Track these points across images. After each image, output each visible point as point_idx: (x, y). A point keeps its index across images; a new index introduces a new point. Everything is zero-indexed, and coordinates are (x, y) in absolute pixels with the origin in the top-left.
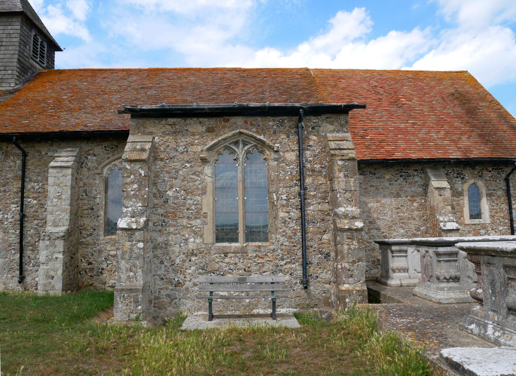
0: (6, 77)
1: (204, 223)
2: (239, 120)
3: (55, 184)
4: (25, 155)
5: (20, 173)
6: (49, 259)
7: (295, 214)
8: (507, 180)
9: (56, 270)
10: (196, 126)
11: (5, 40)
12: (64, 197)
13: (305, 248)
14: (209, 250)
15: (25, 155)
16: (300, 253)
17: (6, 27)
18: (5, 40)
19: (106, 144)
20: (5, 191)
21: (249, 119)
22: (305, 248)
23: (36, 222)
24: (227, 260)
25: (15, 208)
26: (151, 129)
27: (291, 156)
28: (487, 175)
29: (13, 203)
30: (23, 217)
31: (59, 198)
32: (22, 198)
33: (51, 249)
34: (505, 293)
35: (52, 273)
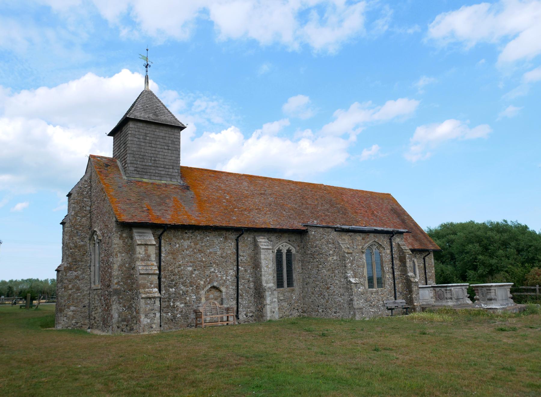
0: (174, 174)
1: (365, 280)
2: (372, 235)
3: (265, 259)
4: (237, 240)
5: (235, 250)
6: (272, 302)
7: (391, 276)
8: (424, 259)
9: (274, 308)
10: (359, 237)
11: (170, 145)
12: (270, 266)
13: (395, 290)
14: (367, 292)
15: (237, 240)
16: (393, 292)
17: (170, 136)
18: (170, 145)
19: (276, 235)
20: (226, 262)
21: (376, 235)
22: (395, 290)
23: (243, 281)
24: (372, 296)
25: (232, 273)
26: (344, 237)
27: (388, 251)
28: (418, 256)
29: (231, 269)
30: (237, 277)
31: (267, 267)
32: (238, 266)
33: (272, 296)
34: (486, 296)
35: (273, 310)
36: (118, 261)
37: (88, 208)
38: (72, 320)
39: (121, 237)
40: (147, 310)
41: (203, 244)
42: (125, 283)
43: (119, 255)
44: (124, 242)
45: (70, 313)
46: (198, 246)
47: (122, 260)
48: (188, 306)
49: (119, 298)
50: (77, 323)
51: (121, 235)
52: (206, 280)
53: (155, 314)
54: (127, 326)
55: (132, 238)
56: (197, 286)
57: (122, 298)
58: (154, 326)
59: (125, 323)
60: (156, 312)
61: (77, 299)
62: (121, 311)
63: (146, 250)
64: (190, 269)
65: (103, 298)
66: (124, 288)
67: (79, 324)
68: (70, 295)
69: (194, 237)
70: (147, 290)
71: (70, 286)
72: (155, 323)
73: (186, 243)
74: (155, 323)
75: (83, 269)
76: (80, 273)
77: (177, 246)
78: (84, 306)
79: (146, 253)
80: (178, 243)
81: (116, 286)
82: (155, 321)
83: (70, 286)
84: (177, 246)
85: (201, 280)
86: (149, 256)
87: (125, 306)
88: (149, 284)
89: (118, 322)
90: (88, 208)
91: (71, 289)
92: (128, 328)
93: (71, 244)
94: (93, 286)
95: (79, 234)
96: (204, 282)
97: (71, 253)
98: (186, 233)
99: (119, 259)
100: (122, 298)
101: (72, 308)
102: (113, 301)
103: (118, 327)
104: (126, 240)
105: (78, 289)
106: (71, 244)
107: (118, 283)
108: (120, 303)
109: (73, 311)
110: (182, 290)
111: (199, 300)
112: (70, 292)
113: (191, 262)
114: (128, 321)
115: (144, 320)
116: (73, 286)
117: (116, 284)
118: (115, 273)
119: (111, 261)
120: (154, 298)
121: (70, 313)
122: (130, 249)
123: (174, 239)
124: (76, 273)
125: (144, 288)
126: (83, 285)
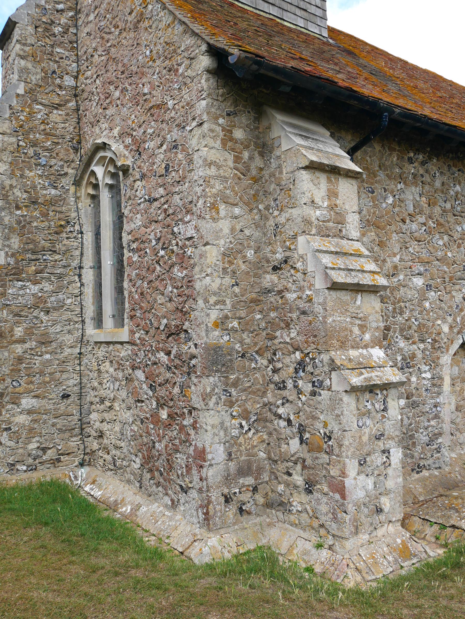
36: (216, 233)
37: (69, 81)
38: (29, 440)
39: (228, 140)
40: (365, 439)
41: (448, 206)
42: (246, 325)
43: (222, 207)
44: (237, 159)
45: (22, 419)
46: (437, 210)
47: (233, 230)
48: (414, 405)
49: (228, 385)
50: (44, 450)
51: (228, 132)
52: (455, 320)
53: (386, 452)
54: (255, 489)
55: (264, 148)
56: (435, 340)
57: (235, 384)
58: (386, 503)
59: (250, 481)
60: (390, 444)
61: (41, 373)
62: (235, 432)
63: (332, 194)
64: (419, 282)
65: (140, 375)
66: (241, 342)
67: (50, 454)
68: (20, 360)
69: (427, 178)
70: (353, 353)
71: (19, 331)
72: (387, 493)
73: (412, 195)
74: (387, 493)
75: (60, 277)
76: (47, 287)
77: (390, 200)
78: (66, 396)
79: (332, 208)
80: (392, 192)
81: (217, 337)
82: (390, 484)
83: (19, 331)
84: (390, 200)
85: (444, 320)
86: (340, 220)
87: (245, 415)
88: (356, 330)
89: (228, 479)
90: (69, 81)
91: (22, 341)
92: (261, 500)
93: (18, 193)
94: (90, 331)
95: (43, 161)
96: (451, 327)
97: (19, 222)
98: (411, 161)
99: (225, 226)
100: (235, 384)
101: (27, 402)
102: (205, 397)
103: (227, 500)
104: (246, 155)
105: (45, 341)
106: (18, 193)
107: (221, 324)
108: (231, 404)
109: (29, 412)
110: (400, 350)
111: (437, 382)
112: (19, 349)
113: (422, 262)
114: (260, 470)
115: (359, 486)
116: (29, 332)
117: (216, 325)
118: (209, 280)
119: (191, 232)
120: (386, 387)
121: (22, 419)
122: (259, 187)
123: (381, 175)
124: (35, 289)
125: (343, 345)
126: (58, 328)
